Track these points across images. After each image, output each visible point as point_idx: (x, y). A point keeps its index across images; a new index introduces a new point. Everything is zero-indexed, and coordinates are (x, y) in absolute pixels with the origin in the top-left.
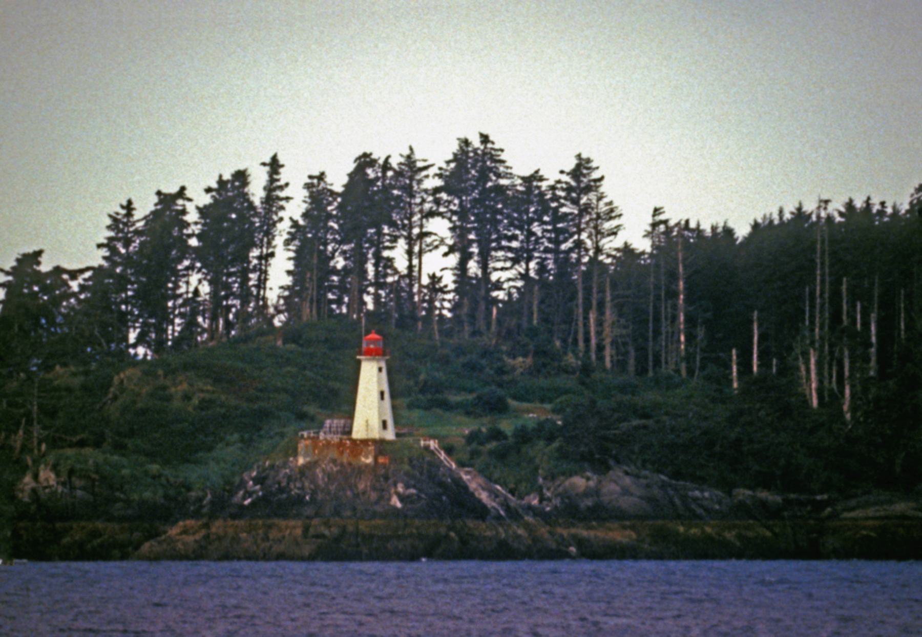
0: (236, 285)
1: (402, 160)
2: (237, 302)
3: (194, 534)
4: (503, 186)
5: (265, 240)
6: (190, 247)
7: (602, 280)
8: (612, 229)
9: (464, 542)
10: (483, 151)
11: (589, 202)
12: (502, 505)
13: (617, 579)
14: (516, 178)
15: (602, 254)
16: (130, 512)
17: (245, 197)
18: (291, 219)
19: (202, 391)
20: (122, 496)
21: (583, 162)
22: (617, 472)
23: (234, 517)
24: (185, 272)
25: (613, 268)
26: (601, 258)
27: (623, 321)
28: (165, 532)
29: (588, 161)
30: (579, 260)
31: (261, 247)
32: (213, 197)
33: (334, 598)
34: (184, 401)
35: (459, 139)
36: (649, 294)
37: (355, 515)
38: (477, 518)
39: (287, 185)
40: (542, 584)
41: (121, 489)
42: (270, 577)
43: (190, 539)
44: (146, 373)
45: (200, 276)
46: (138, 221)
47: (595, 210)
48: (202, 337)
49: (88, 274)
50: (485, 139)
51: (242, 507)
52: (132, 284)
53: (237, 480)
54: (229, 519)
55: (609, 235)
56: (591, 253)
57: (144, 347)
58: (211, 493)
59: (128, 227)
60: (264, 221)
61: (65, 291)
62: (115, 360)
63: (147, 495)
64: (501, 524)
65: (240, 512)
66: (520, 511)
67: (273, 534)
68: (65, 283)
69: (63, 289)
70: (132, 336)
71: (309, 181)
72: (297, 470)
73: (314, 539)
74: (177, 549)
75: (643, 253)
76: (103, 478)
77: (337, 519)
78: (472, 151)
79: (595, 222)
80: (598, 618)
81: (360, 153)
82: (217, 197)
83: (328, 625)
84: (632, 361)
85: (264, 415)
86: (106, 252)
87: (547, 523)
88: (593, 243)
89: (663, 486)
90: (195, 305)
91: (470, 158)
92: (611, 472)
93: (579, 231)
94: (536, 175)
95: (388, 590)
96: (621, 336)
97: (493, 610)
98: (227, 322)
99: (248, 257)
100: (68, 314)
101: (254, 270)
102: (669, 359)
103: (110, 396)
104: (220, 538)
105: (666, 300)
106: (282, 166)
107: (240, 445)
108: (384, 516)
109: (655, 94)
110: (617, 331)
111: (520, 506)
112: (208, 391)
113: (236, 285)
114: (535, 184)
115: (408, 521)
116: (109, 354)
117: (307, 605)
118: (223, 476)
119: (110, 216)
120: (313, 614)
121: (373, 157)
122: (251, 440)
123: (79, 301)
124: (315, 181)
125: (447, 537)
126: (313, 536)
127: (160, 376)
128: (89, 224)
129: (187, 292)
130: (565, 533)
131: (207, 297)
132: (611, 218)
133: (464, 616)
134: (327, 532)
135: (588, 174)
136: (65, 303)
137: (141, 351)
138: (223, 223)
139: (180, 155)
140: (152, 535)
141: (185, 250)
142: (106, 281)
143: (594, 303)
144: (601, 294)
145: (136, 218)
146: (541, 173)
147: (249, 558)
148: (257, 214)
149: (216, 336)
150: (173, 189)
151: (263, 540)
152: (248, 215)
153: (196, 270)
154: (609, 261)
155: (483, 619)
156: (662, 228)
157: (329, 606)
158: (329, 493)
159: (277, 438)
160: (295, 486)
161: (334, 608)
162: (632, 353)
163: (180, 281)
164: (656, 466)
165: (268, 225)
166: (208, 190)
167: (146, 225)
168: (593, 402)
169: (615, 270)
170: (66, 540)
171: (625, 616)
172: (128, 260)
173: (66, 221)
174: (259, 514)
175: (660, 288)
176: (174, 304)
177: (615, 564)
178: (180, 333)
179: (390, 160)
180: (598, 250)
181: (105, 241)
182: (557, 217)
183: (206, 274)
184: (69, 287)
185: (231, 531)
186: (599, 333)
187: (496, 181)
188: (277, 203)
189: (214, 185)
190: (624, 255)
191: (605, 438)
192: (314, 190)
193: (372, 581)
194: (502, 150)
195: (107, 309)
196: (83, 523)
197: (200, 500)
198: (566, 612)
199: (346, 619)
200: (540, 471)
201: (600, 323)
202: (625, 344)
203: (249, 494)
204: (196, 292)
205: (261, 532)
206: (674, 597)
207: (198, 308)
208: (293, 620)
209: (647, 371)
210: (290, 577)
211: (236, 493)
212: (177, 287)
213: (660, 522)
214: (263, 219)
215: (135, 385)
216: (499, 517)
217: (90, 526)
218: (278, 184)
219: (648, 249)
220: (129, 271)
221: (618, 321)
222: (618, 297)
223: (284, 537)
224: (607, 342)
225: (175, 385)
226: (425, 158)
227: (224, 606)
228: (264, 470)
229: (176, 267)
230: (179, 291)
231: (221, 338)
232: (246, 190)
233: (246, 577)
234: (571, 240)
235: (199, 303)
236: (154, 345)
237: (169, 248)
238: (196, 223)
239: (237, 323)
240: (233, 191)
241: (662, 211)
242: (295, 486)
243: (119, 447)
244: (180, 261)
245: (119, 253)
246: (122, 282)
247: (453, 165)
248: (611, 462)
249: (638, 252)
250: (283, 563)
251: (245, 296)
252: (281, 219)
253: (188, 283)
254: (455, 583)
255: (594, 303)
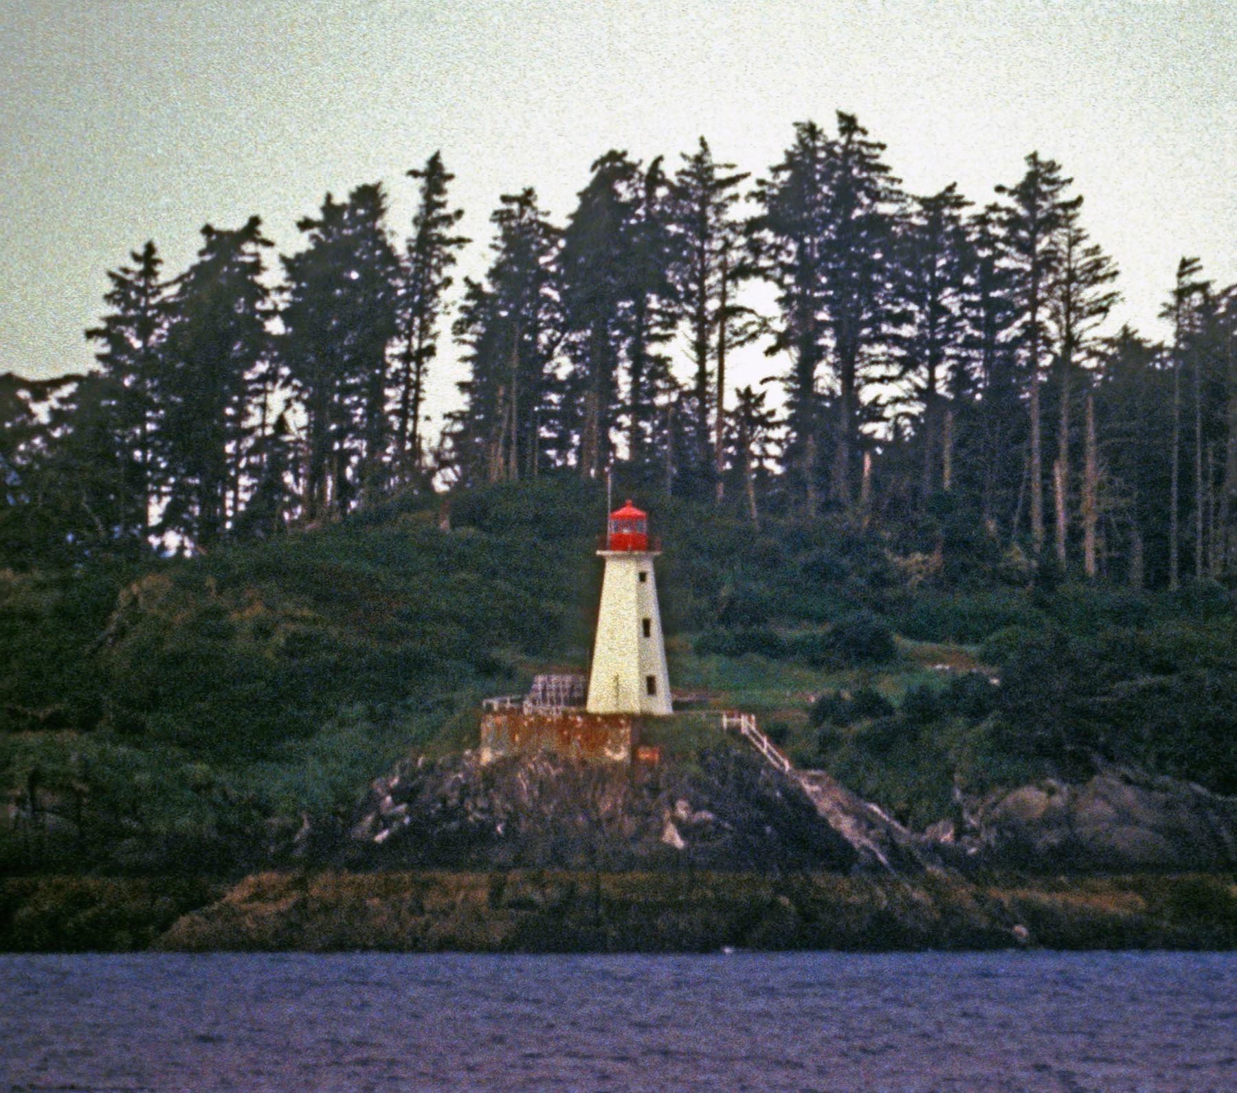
0: (360, 411)
1: (686, 166)
2: (361, 445)
3: (276, 900)
4: (885, 216)
5: (417, 322)
6: (269, 335)
7: (1079, 400)
8: (1098, 301)
9: (806, 917)
10: (845, 147)
11: (1052, 247)
12: (882, 843)
13: (1110, 989)
14: (909, 200)
15: (1079, 351)
16: (151, 857)
17: (377, 238)
18: (467, 280)
19: (293, 619)
20: (135, 825)
21: (1042, 170)
22: (1107, 779)
23: (354, 866)
24: (260, 386)
25: (1100, 377)
26: (1076, 358)
27: (1119, 481)
28: (219, 897)
29: (1052, 167)
30: (1032, 362)
31: (409, 337)
32: (313, 237)
33: (551, 1026)
34: (257, 639)
35: (796, 124)
36: (1171, 430)
37: (593, 862)
38: (833, 868)
39: (459, 214)
40: (959, 997)
41: (133, 811)
42: (426, 983)
43: (269, 909)
44: (182, 584)
45: (288, 393)
46: (167, 285)
47: (1066, 264)
48: (292, 514)
49: (68, 390)
50: (848, 124)
51: (370, 846)
52: (155, 408)
53: (361, 794)
54: (346, 870)
55: (1092, 313)
56: (1057, 348)
57: (178, 532)
58: (309, 819)
59: (147, 296)
60: (414, 286)
61: (24, 423)
62: (122, 558)
63: (185, 822)
64: (879, 882)
65: (368, 857)
66: (917, 854)
67: (433, 900)
68: (23, 408)
69: (18, 420)
70: (155, 512)
71: (503, 207)
72: (479, 773)
73: (513, 911)
74: (244, 929)
75: (1159, 348)
76: (99, 790)
77: (557, 870)
78: (823, 148)
79: (1064, 287)
80: (1071, 1065)
81: (604, 152)
82: (322, 237)
83: (541, 1080)
84: (1137, 561)
85: (414, 666)
86: (103, 346)
87: (971, 879)
88: (1061, 330)
89: (1199, 806)
90: (277, 450)
91: (820, 161)
92: (1096, 778)
93: (1034, 306)
94: (948, 195)
95: (658, 1010)
96: (1116, 511)
97: (864, 1050)
98: (342, 484)
99: (383, 355)
100: (30, 466)
101: (395, 382)
102: (1211, 555)
103: (112, 628)
104: (327, 909)
105: (1204, 441)
106: (451, 177)
107: (366, 725)
108: (648, 866)
109: (1182, 35)
110: (1109, 502)
111: (917, 845)
112: (303, 619)
113: (360, 411)
114: (946, 212)
115: (698, 874)
116: (109, 545)
117: (500, 1040)
118: (333, 786)
119: (112, 275)
120: (510, 1057)
121: (628, 159)
122: (389, 715)
123: (51, 442)
124: (515, 207)
125: (773, 905)
126: (510, 905)
127: (210, 589)
128: (69, 291)
129: (263, 425)
130: (1006, 898)
131: (303, 434)
132: (1096, 280)
133: (807, 1062)
134: (537, 897)
135: (1052, 193)
136: (22, 447)
137: (172, 540)
138: (334, 290)
139: (249, 155)
140: (194, 902)
141: (260, 343)
142: (104, 403)
143: (1064, 446)
144: (1076, 429)
145: (162, 279)
146: (958, 191)
147: (384, 948)
148: (400, 272)
149: (318, 513)
150: (237, 223)
151: (412, 912)
152: (382, 274)
153: (280, 382)
154: (1092, 363)
155: (844, 1067)
156: (1197, 298)
157: (542, 1042)
158: (542, 819)
159: (440, 711)
160: (475, 806)
161: (552, 1046)
162: (1138, 545)
163: (250, 402)
164: (1186, 767)
165: (422, 293)
166: (305, 225)
167: (182, 292)
168: (1061, 641)
169: (1104, 381)
170: (24, 912)
171: (1124, 1061)
172: (146, 362)
173: (25, 284)
174: (405, 860)
175: (1193, 418)
176: (237, 448)
177: (1105, 958)
178: (247, 504)
179: (663, 166)
180: (1071, 343)
181: (103, 325)
182: (991, 279)
183: (301, 390)
184: (32, 415)
185: (348, 894)
186: (1072, 506)
187: (870, 206)
188: (439, 249)
189: (317, 216)
190: (1122, 353)
191: (1084, 712)
192: (513, 224)
193: (627, 992)
194: (882, 147)
195: (106, 457)
196: (58, 879)
197: (289, 832)
198: (1008, 1052)
199: (576, 1067)
200: (957, 777)
201: (1074, 486)
202: (1122, 526)
203: (383, 821)
204: (281, 425)
205: (407, 895)
206: (1219, 1023)
207: (285, 456)
208: (471, 1069)
209: (1166, 580)
210: (466, 984)
211: (360, 819)
212: (243, 414)
213: (1192, 877)
214: (412, 282)
215: (161, 607)
216: (876, 867)
217: (73, 884)
218: (442, 212)
219: (1170, 342)
220: (149, 384)
221: (1111, 482)
222: (1111, 433)
223: (453, 907)
224: (1089, 522)
225: (240, 607)
226: (731, 162)
227: (336, 1042)
228: (415, 775)
229: (242, 374)
230: (247, 424)
231: (330, 514)
232: (379, 224)
233: (379, 984)
234: (1018, 323)
235: (286, 447)
236: (199, 529)
237: (226, 339)
238: (281, 290)
239: (361, 486)
240: (352, 227)
241: (1196, 265)
242: (475, 806)
243: (129, 730)
244: (250, 365)
245: (129, 349)
246: (135, 405)
247: (785, 175)
248: (1097, 759)
249: (1149, 345)
250: (450, 957)
251: (377, 433)
252: (448, 282)
253: (264, 407)
254: (789, 995)
255: (1064, 446)
